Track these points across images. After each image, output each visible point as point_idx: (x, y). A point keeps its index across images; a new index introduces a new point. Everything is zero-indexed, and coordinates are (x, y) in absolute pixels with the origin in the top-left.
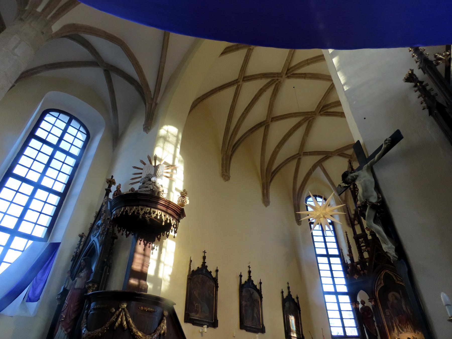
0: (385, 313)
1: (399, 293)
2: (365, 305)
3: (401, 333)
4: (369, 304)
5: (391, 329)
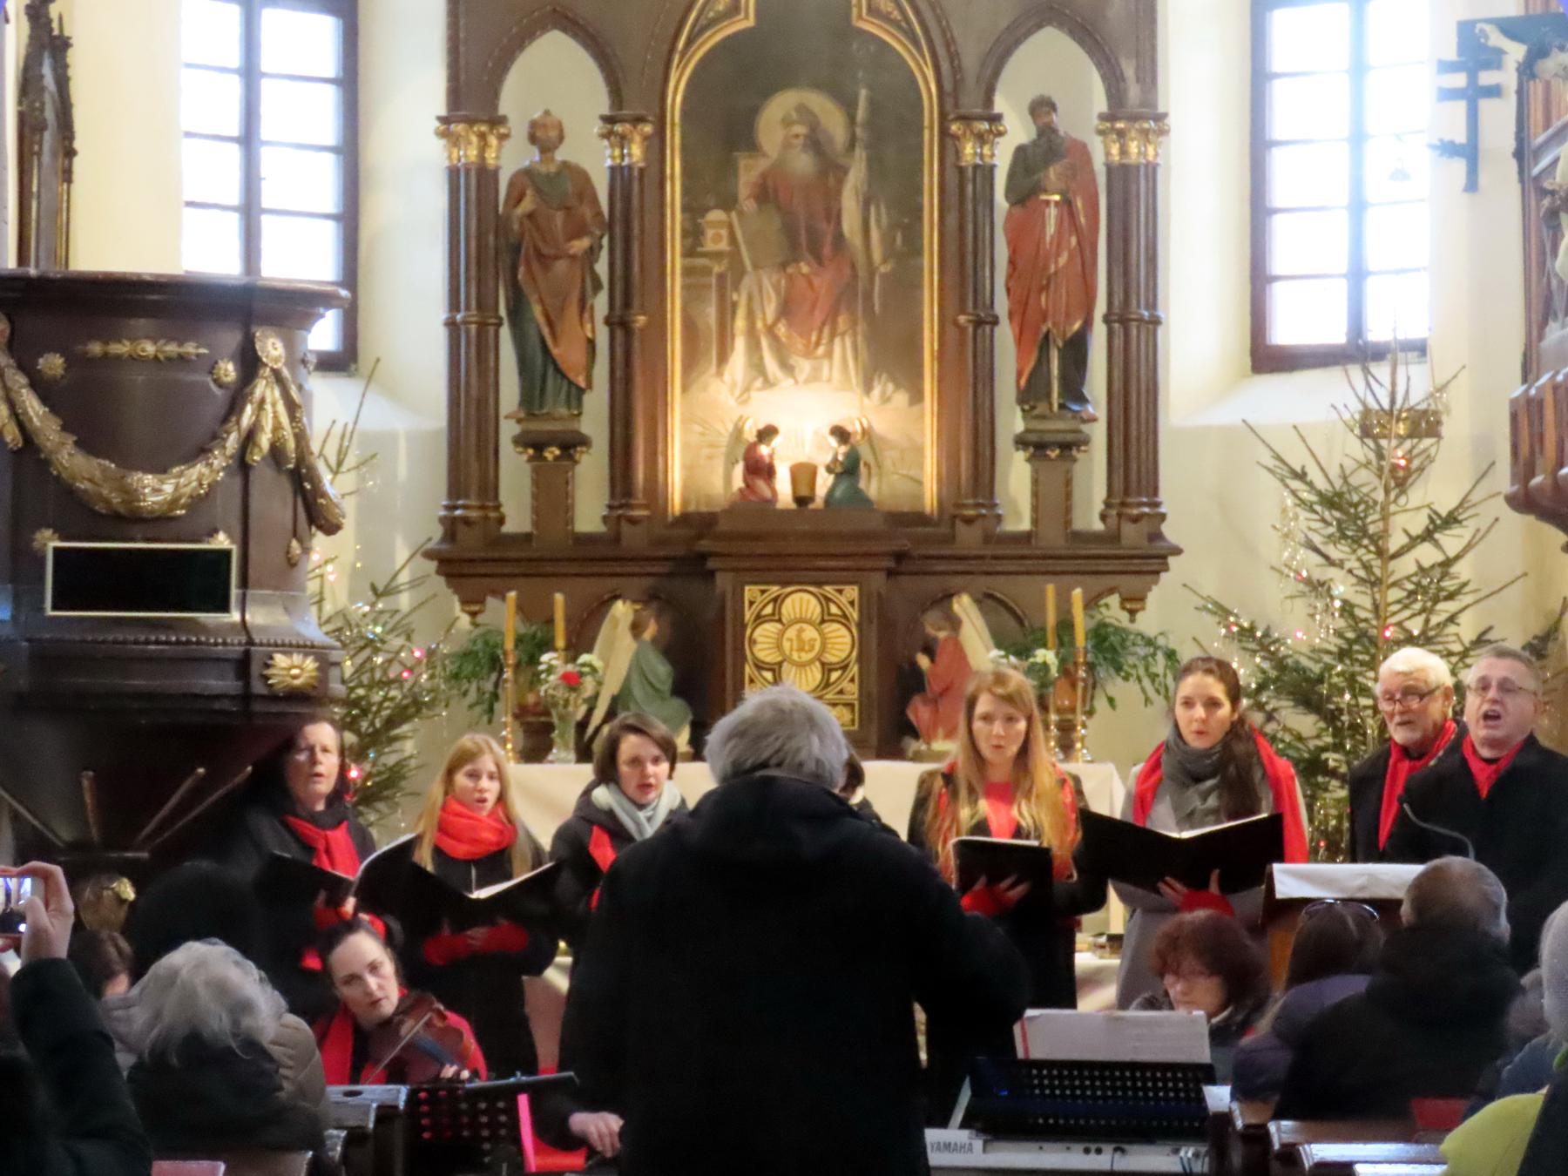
0: (693, 234)
1: (849, 106)
2: (560, 155)
3: (768, 383)
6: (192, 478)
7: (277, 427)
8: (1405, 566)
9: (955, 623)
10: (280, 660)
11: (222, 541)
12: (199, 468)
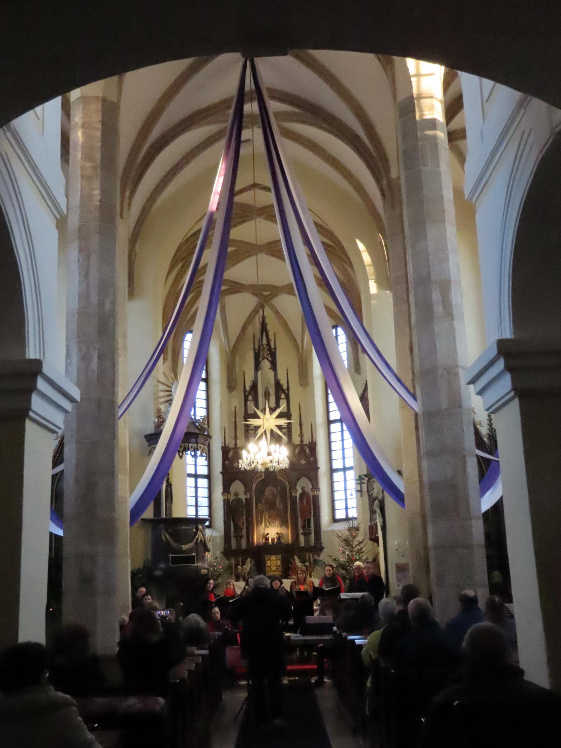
0: (257, 507)
3: (268, 527)
4: (243, 497)
5: (259, 522)
6: (190, 545)
7: (201, 538)
8: (356, 549)
9: (294, 560)
10: (202, 571)
11: (194, 554)
12: (191, 544)
